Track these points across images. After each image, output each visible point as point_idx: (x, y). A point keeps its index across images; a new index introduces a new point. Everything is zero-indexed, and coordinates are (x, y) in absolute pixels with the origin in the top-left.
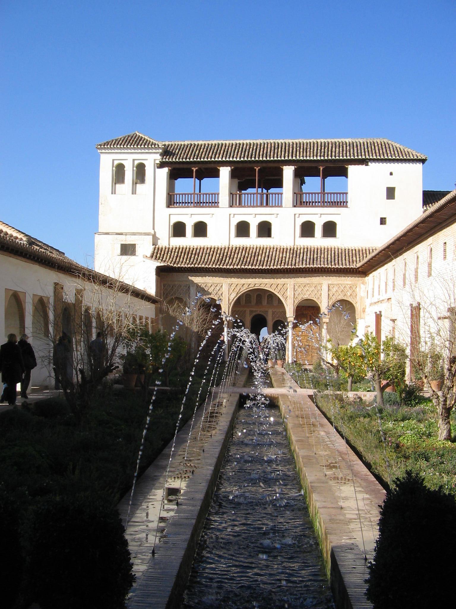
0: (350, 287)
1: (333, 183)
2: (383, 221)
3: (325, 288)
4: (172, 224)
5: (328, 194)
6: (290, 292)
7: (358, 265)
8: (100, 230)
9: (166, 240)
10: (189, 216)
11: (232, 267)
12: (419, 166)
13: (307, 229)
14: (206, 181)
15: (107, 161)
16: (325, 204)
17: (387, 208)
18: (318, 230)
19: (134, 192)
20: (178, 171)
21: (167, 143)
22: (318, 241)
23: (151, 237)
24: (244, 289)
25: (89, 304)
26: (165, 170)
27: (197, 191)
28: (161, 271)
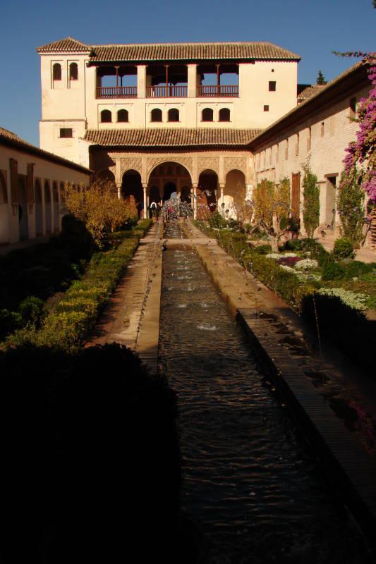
0: (241, 160)
1: (226, 78)
2: (266, 108)
3: (221, 160)
4: (100, 112)
5: (223, 87)
6: (195, 164)
7: (248, 142)
8: (44, 118)
9: (96, 124)
10: (114, 106)
11: (148, 145)
12: (294, 65)
13: (207, 115)
14: (126, 77)
15: (47, 62)
16: (219, 94)
17: (269, 98)
18: (216, 116)
19: (68, 87)
20: (103, 69)
21: (94, 47)
22: (216, 124)
23: (84, 123)
24: (159, 163)
25: (39, 176)
26: (93, 69)
27: (119, 85)
28: (92, 150)
